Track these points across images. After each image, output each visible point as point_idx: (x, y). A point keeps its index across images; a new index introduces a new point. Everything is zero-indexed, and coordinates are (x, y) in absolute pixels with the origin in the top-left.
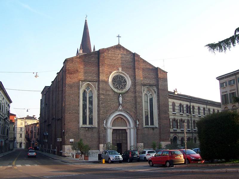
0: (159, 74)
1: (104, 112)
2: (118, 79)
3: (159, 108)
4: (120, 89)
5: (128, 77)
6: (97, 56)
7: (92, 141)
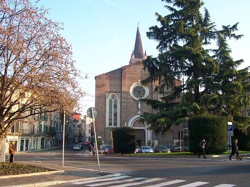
4: (139, 97)
6: (120, 72)
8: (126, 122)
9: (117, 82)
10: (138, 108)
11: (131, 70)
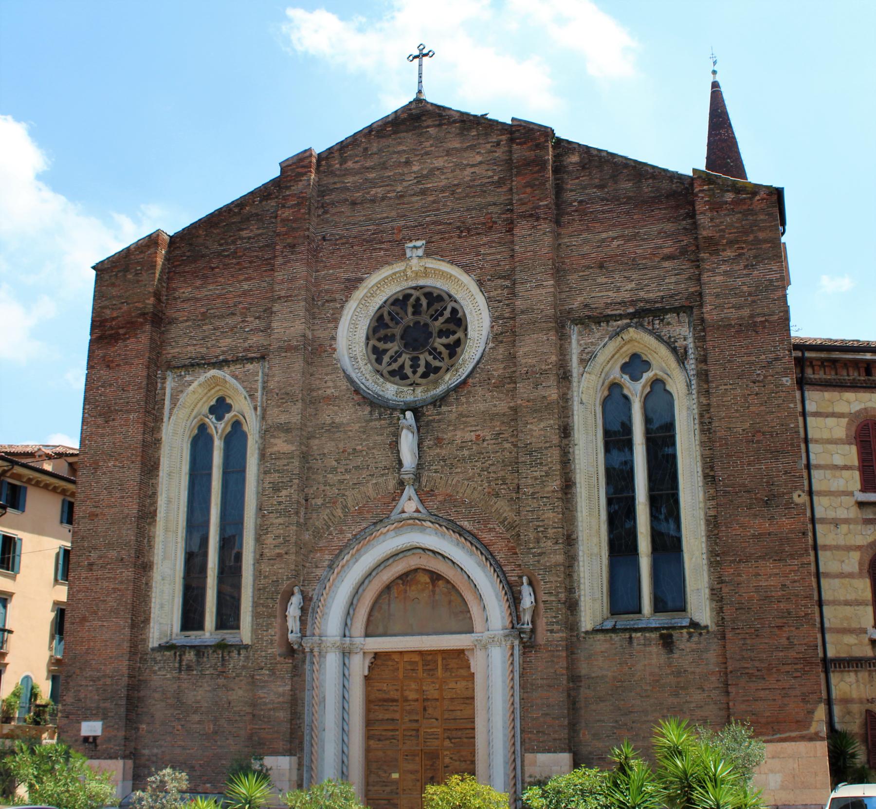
0: (703, 220)
1: (286, 541)
4: (417, 378)
5: (474, 288)
7: (216, 732)
8: (296, 600)
9: (246, 286)
10: (400, 463)
11: (349, 180)
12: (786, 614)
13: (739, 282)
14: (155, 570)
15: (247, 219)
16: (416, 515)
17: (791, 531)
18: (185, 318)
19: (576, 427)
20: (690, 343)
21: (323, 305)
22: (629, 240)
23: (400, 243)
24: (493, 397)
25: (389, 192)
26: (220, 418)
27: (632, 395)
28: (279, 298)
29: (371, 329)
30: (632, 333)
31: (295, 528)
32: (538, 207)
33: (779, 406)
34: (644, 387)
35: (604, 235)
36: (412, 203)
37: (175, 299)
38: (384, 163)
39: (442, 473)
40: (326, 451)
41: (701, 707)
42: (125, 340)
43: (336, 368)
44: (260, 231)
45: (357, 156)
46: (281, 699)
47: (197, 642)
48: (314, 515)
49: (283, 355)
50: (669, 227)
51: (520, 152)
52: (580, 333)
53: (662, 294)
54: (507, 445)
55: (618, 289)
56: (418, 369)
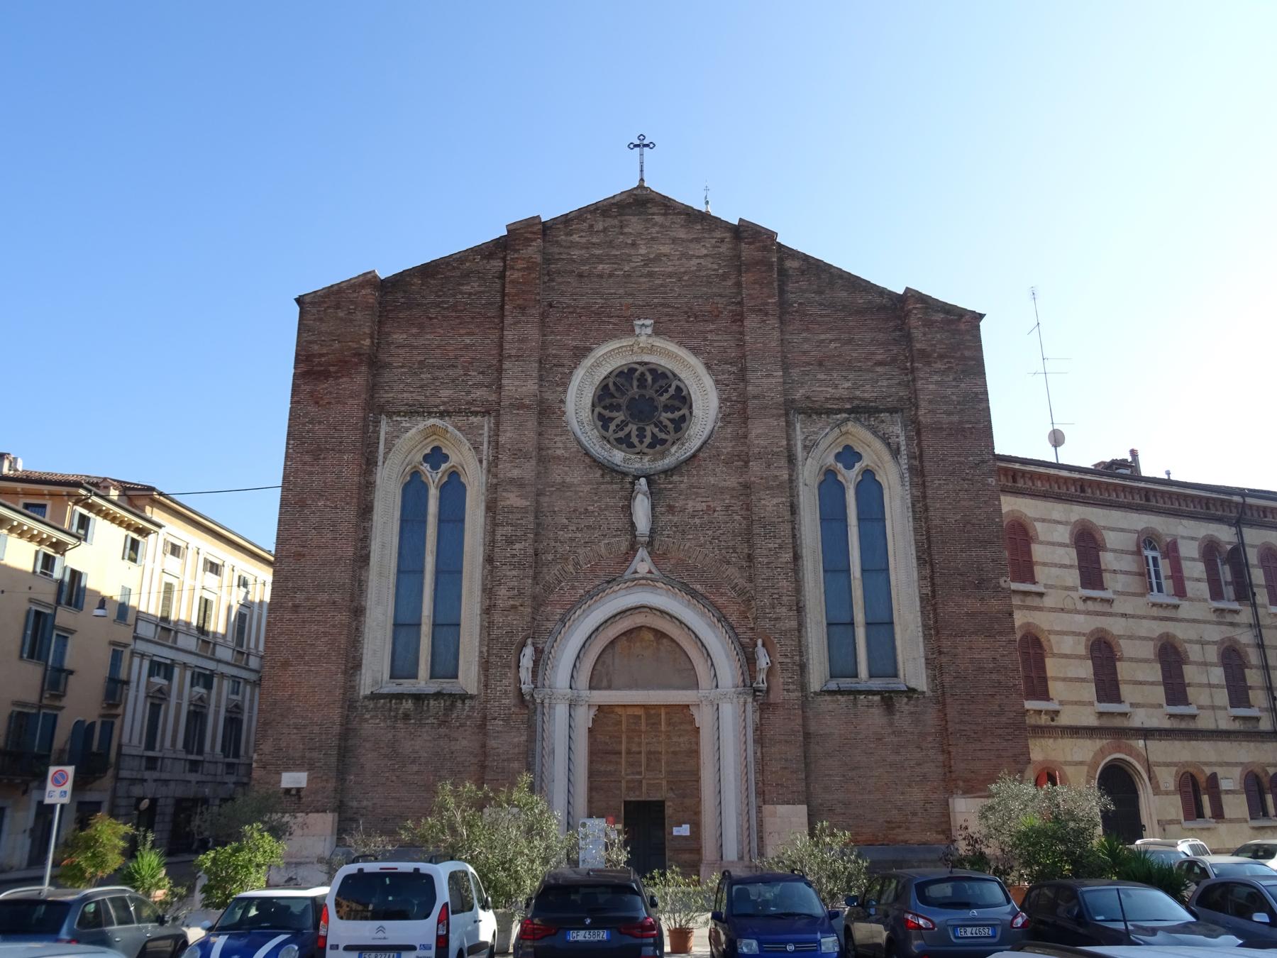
0: (917, 334)
2: (635, 390)
3: (930, 555)
4: (643, 447)
8: (529, 651)
10: (633, 525)
11: (576, 253)
12: (996, 685)
13: (949, 391)
14: (367, 615)
15: (466, 275)
16: (649, 575)
17: (998, 612)
18: (400, 364)
19: (801, 506)
20: (902, 440)
21: (551, 369)
22: (845, 344)
23: (629, 320)
24: (722, 472)
25: (616, 270)
26: (435, 467)
27: (847, 481)
28: (510, 356)
29: (596, 398)
30: (850, 426)
31: (530, 581)
32: (767, 304)
33: (985, 502)
34: (857, 475)
35: (823, 337)
36: (640, 283)
37: (389, 344)
38: (611, 242)
39: (674, 538)
40: (556, 509)
41: (920, 764)
42: (338, 378)
43: (565, 430)
44: (482, 289)
45: (582, 231)
46: (516, 750)
47: (414, 690)
48: (545, 570)
49: (515, 412)
50: (881, 336)
51: (747, 251)
52: (803, 422)
53: (875, 394)
54: (737, 518)
55: (836, 387)
56: (644, 440)
